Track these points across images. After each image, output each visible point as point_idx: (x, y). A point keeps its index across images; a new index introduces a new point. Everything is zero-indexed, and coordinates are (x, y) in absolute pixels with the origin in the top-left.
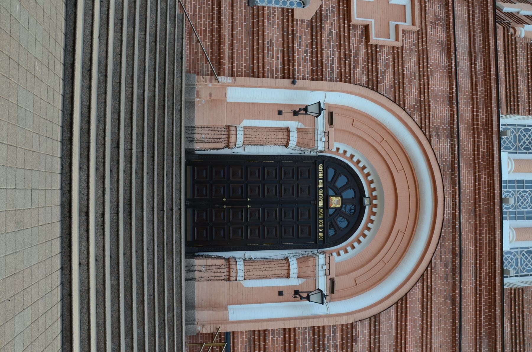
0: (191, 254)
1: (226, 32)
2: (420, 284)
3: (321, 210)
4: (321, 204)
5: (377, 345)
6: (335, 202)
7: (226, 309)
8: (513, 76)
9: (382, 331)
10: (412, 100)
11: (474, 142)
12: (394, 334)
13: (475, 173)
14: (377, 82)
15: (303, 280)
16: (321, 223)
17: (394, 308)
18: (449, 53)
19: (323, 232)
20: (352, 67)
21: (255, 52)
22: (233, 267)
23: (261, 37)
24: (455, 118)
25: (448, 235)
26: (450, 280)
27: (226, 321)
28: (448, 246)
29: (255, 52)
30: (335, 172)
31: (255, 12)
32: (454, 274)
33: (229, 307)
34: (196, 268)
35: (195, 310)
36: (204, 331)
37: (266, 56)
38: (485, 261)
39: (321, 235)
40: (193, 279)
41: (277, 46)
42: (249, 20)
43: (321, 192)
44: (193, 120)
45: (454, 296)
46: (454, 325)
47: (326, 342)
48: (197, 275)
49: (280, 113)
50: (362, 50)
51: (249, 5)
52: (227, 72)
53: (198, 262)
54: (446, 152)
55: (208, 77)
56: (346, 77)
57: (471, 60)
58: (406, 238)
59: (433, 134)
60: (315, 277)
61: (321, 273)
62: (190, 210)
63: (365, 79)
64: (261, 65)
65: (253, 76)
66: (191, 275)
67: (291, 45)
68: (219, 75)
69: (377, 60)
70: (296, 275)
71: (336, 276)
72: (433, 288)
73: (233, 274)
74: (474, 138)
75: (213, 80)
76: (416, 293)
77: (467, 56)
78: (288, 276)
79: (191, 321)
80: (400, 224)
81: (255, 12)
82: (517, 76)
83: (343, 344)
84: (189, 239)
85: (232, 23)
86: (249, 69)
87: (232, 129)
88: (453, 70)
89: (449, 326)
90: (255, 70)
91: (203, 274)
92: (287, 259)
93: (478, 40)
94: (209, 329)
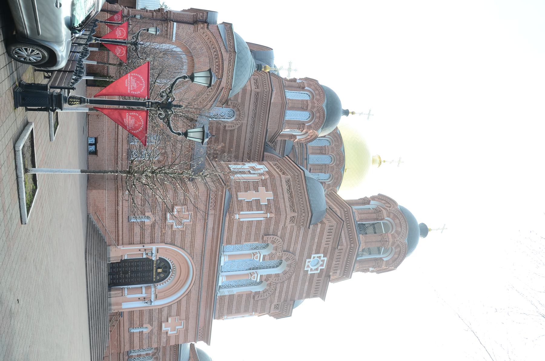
0: (110, 290)
1: (120, 233)
2: (186, 296)
3: (155, 273)
4: (155, 271)
5: (170, 312)
6: (160, 270)
7: (121, 304)
8: (231, 233)
9: (172, 309)
10: (188, 244)
11: (211, 256)
12: (176, 309)
13: (210, 265)
14: (175, 241)
15: (147, 295)
16: (154, 276)
17: (177, 303)
18: (204, 229)
19: (155, 279)
20: (166, 237)
21: (131, 237)
22: (124, 293)
23: (133, 231)
24: (204, 250)
25: (197, 282)
26: (197, 295)
27: (122, 309)
28: (198, 286)
29: (131, 237)
30: (160, 261)
31: (131, 224)
32: (199, 293)
33: (122, 303)
34: (111, 294)
35: (111, 306)
36: (114, 312)
37: (134, 237)
38: (210, 290)
39: (154, 280)
40: (111, 297)
41: (139, 234)
42: (128, 227)
43: (155, 268)
44: (110, 255)
45: (198, 299)
46: (198, 306)
47: (153, 312)
48: (112, 296)
49: (140, 250)
50: (170, 232)
51: (128, 222)
52: (121, 244)
53: (112, 293)
54: (199, 259)
55: (114, 247)
56: (163, 241)
57: (213, 230)
58: (183, 282)
59: (195, 254)
60: (151, 294)
61: (153, 293)
62: (109, 276)
63: (170, 240)
64: (133, 240)
65: (130, 244)
66: (110, 296)
67: (143, 233)
68: (118, 245)
69: (175, 234)
70: (145, 293)
71: (158, 293)
72: (191, 297)
73: (124, 295)
74: (211, 254)
75: (116, 247)
76: (185, 298)
77: (212, 229)
78: (142, 293)
79: (110, 310)
80: (182, 278)
81: (131, 224)
82: (232, 233)
83: (159, 312)
84: (109, 272)
85: (123, 228)
86: (128, 242)
87: (123, 256)
88: (205, 235)
89: (196, 307)
90: (131, 242)
91: (114, 296)
92: (142, 287)
93: (216, 223)
94: (116, 311)
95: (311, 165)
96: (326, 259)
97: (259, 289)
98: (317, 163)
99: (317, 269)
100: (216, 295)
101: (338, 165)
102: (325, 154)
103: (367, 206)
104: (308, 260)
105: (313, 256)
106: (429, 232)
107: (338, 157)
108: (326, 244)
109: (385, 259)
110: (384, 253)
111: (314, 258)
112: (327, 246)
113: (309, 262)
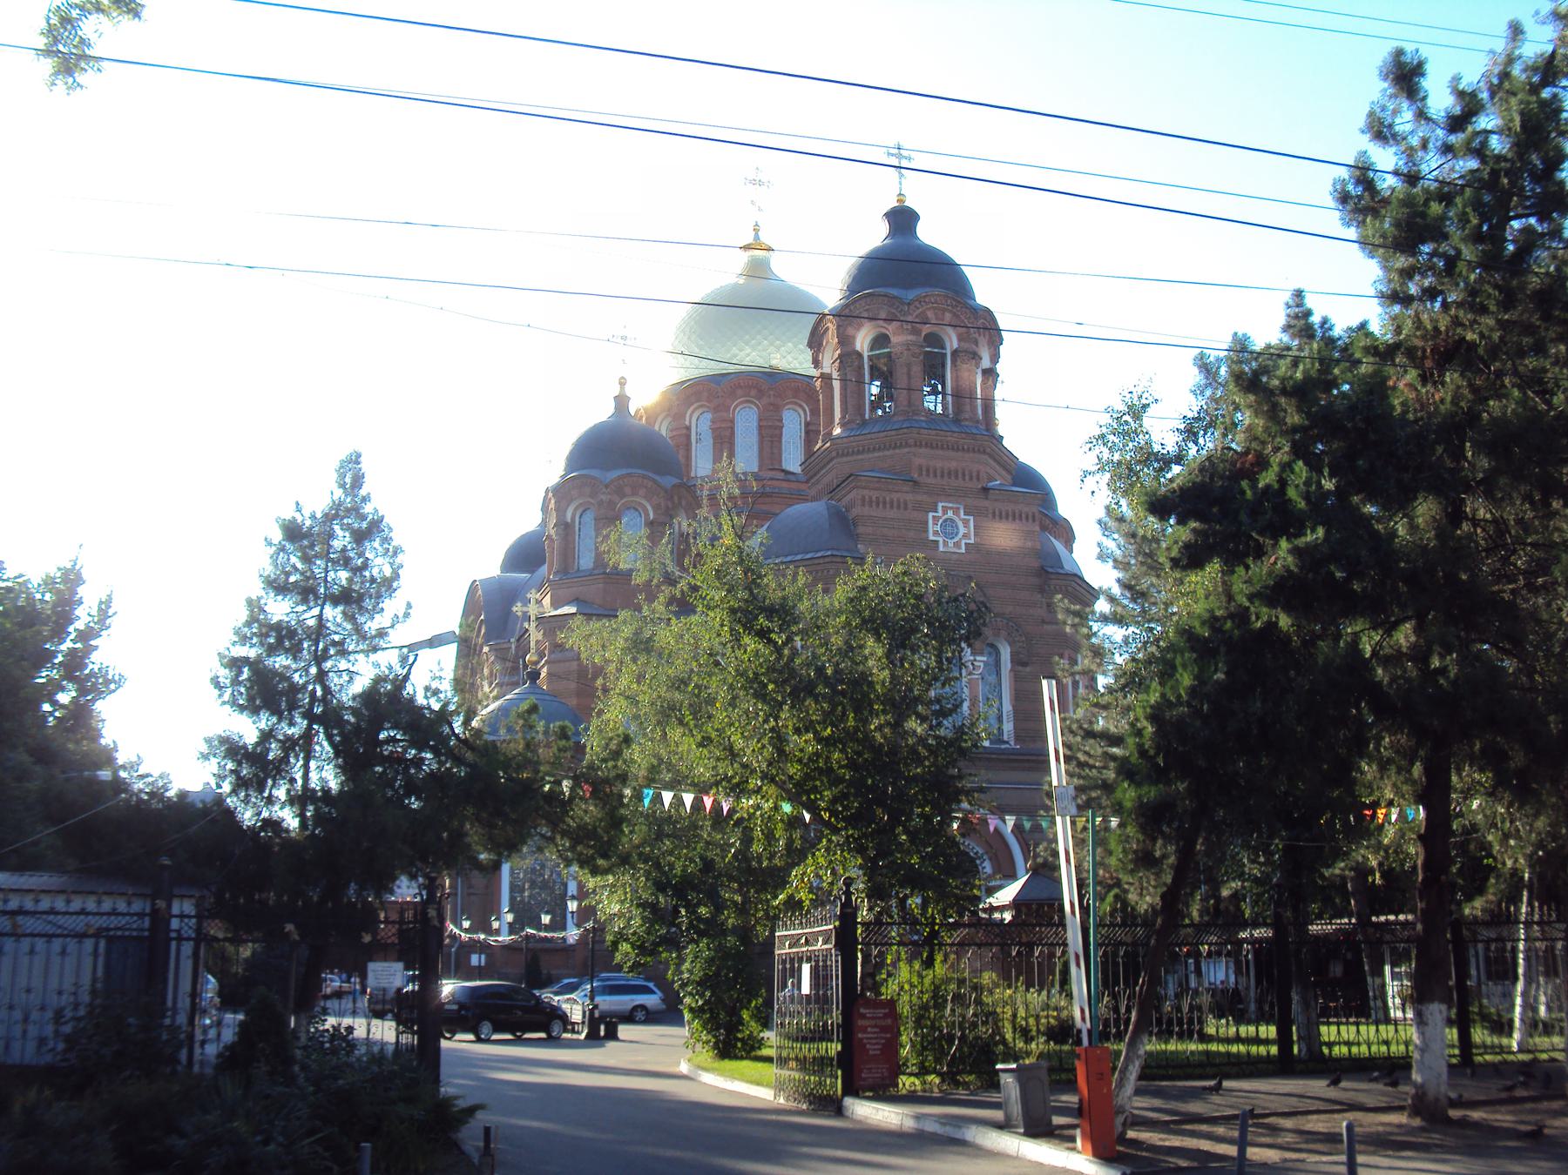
95: (761, 467)
96: (940, 505)
97: (1006, 653)
98: (756, 448)
99: (966, 523)
100: (1013, 752)
101: (760, 391)
102: (732, 429)
103: (836, 385)
104: (941, 549)
105: (932, 537)
106: (910, 203)
107: (739, 392)
108: (906, 509)
109: (955, 345)
110: (943, 348)
111: (936, 533)
112: (910, 506)
113: (945, 544)
